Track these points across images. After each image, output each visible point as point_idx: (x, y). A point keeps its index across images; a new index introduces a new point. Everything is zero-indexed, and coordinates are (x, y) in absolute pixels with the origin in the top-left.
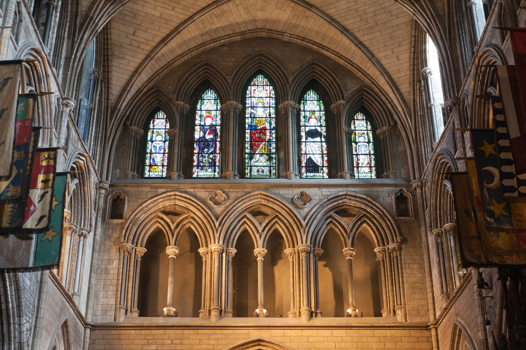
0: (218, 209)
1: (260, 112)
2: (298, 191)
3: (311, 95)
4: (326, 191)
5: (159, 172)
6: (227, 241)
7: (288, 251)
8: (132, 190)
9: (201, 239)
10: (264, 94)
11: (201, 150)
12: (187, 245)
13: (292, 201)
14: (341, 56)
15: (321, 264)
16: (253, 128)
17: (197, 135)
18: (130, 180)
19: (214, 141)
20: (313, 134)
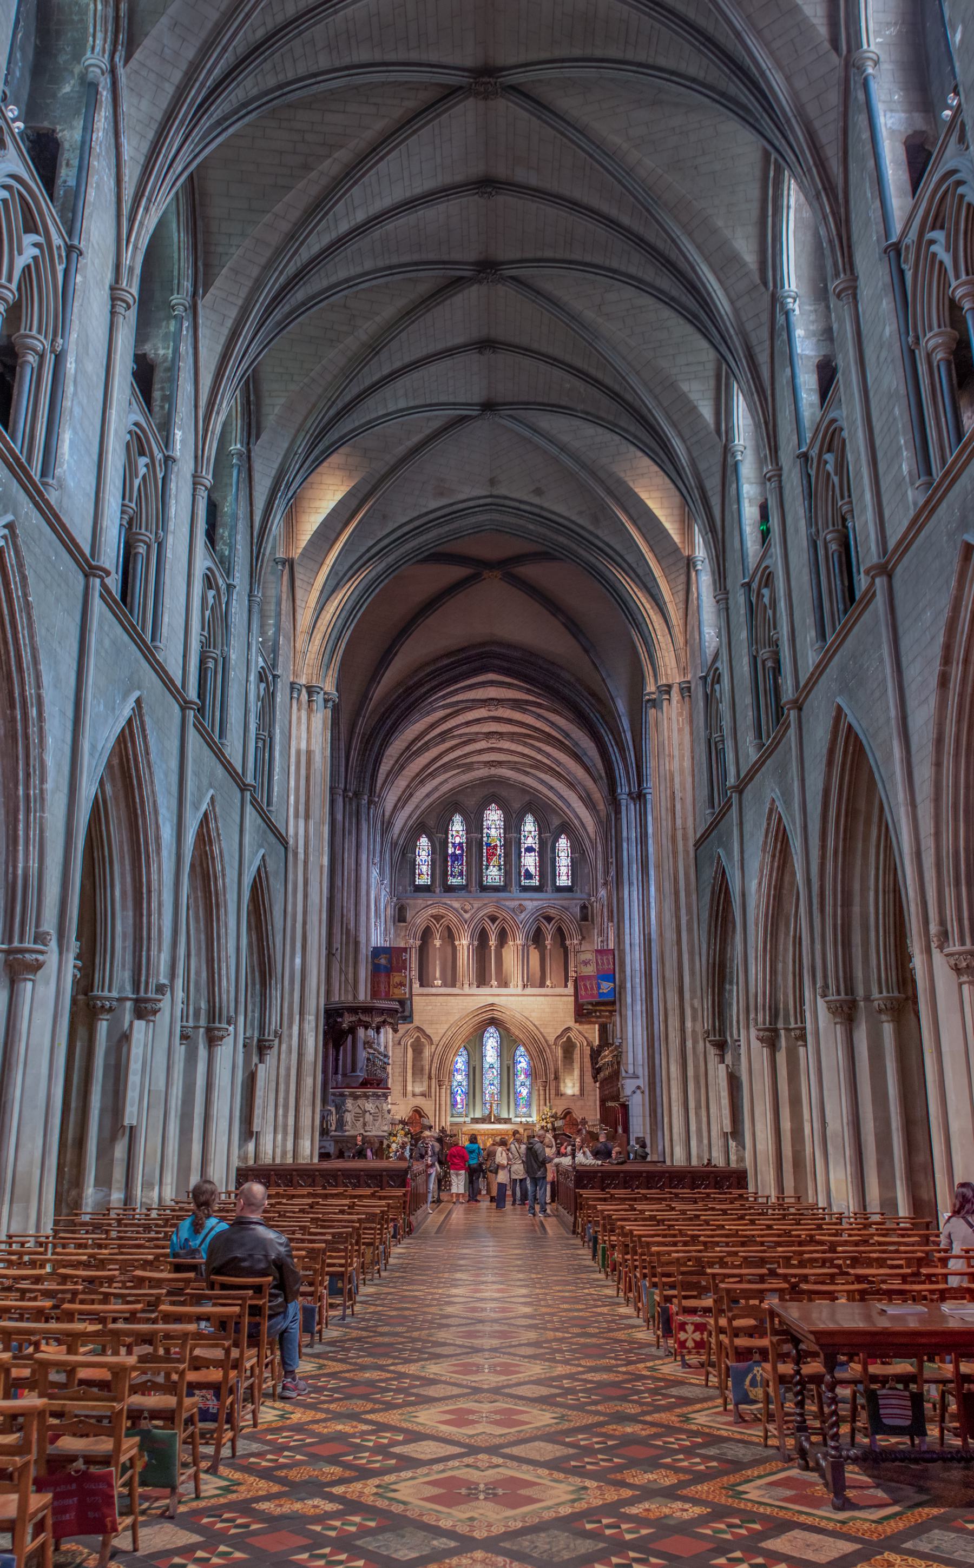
0: (467, 916)
1: (493, 832)
2: (517, 903)
3: (529, 819)
4: (536, 903)
5: (424, 879)
6: (472, 937)
7: (511, 943)
8: (411, 902)
9: (456, 936)
10: (496, 817)
11: (453, 862)
12: (446, 934)
13: (513, 910)
14: (549, 799)
15: (532, 948)
16: (488, 845)
17: (450, 851)
18: (408, 894)
19: (462, 855)
20: (530, 850)
